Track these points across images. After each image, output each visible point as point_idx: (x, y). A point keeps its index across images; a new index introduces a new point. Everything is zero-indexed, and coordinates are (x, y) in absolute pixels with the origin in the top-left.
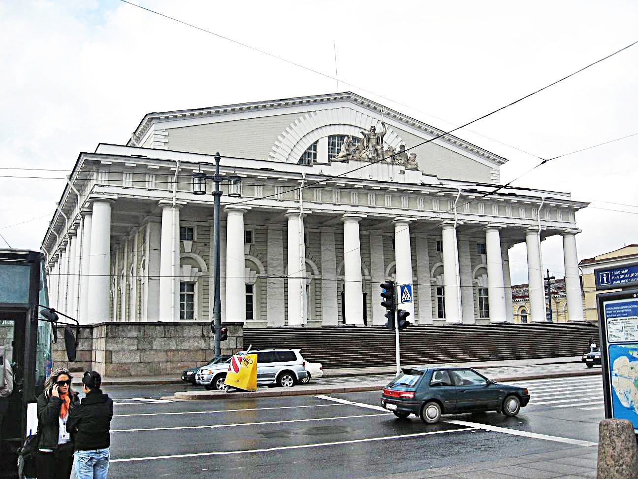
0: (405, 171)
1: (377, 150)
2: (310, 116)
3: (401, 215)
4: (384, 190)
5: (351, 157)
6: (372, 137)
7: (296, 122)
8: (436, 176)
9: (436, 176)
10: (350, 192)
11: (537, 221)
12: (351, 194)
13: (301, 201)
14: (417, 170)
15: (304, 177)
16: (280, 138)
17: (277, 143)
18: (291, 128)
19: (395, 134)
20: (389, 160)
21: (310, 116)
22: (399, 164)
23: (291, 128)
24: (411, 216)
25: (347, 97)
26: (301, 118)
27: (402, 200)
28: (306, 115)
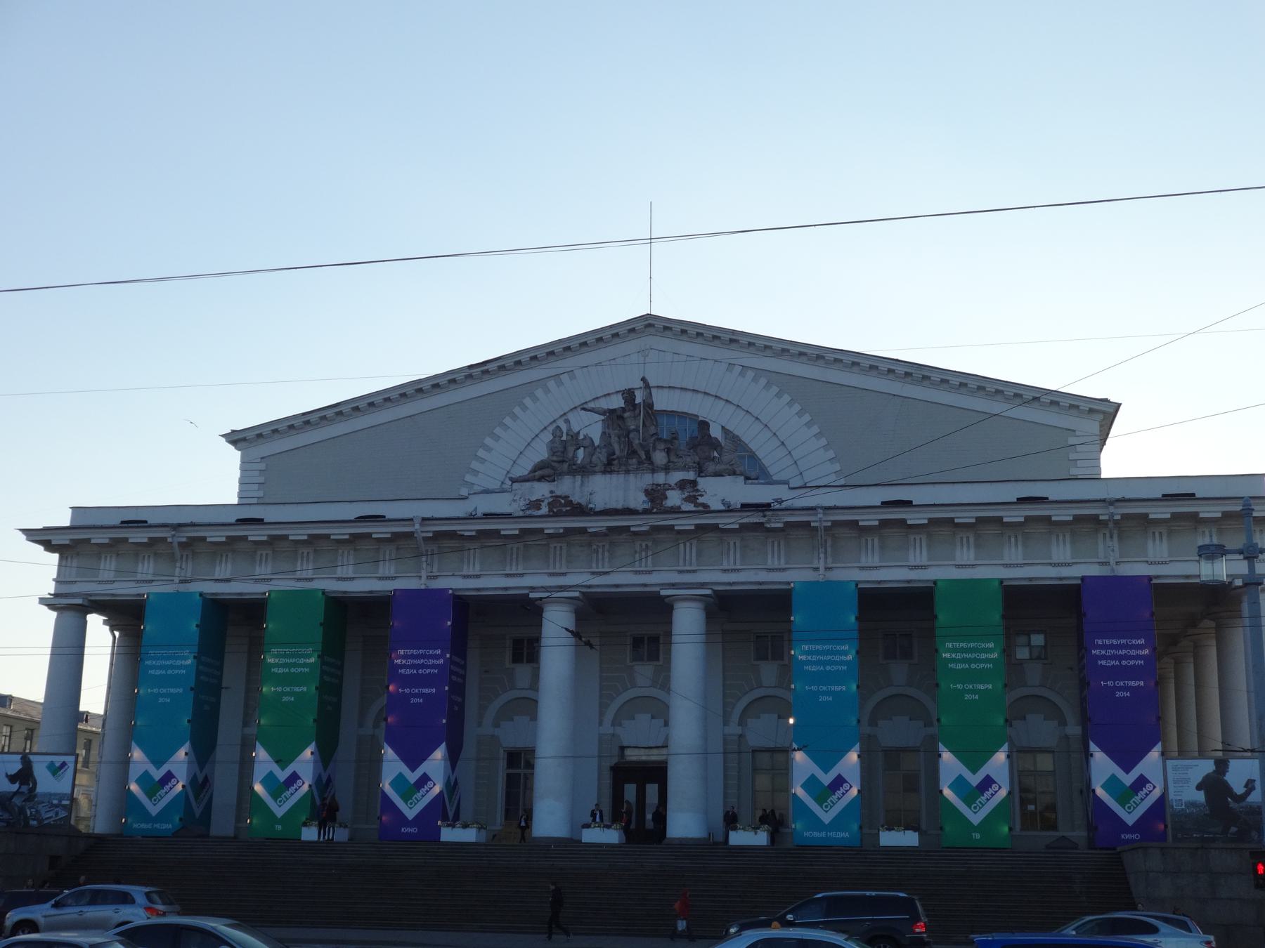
0: (699, 480)
1: (630, 443)
2: (560, 383)
3: (673, 586)
4: (617, 534)
5: (565, 466)
6: (626, 415)
7: (528, 401)
8: (786, 482)
9: (786, 482)
10: (548, 545)
11: (1107, 564)
12: (552, 550)
13: (424, 574)
14: (734, 473)
15: (417, 526)
16: (488, 441)
17: (481, 453)
18: (515, 417)
19: (775, 389)
20: (659, 457)
21: (560, 383)
22: (685, 468)
23: (515, 417)
24: (702, 585)
25: (648, 325)
26: (539, 393)
27: (682, 546)
28: (551, 384)
